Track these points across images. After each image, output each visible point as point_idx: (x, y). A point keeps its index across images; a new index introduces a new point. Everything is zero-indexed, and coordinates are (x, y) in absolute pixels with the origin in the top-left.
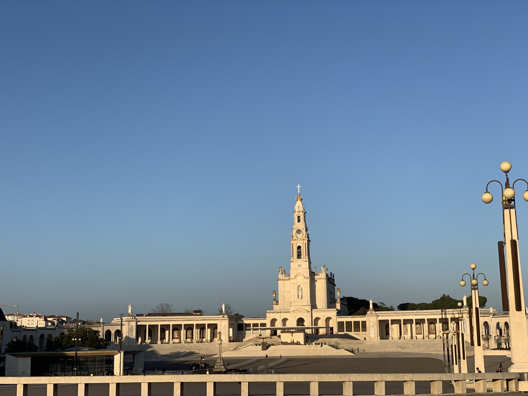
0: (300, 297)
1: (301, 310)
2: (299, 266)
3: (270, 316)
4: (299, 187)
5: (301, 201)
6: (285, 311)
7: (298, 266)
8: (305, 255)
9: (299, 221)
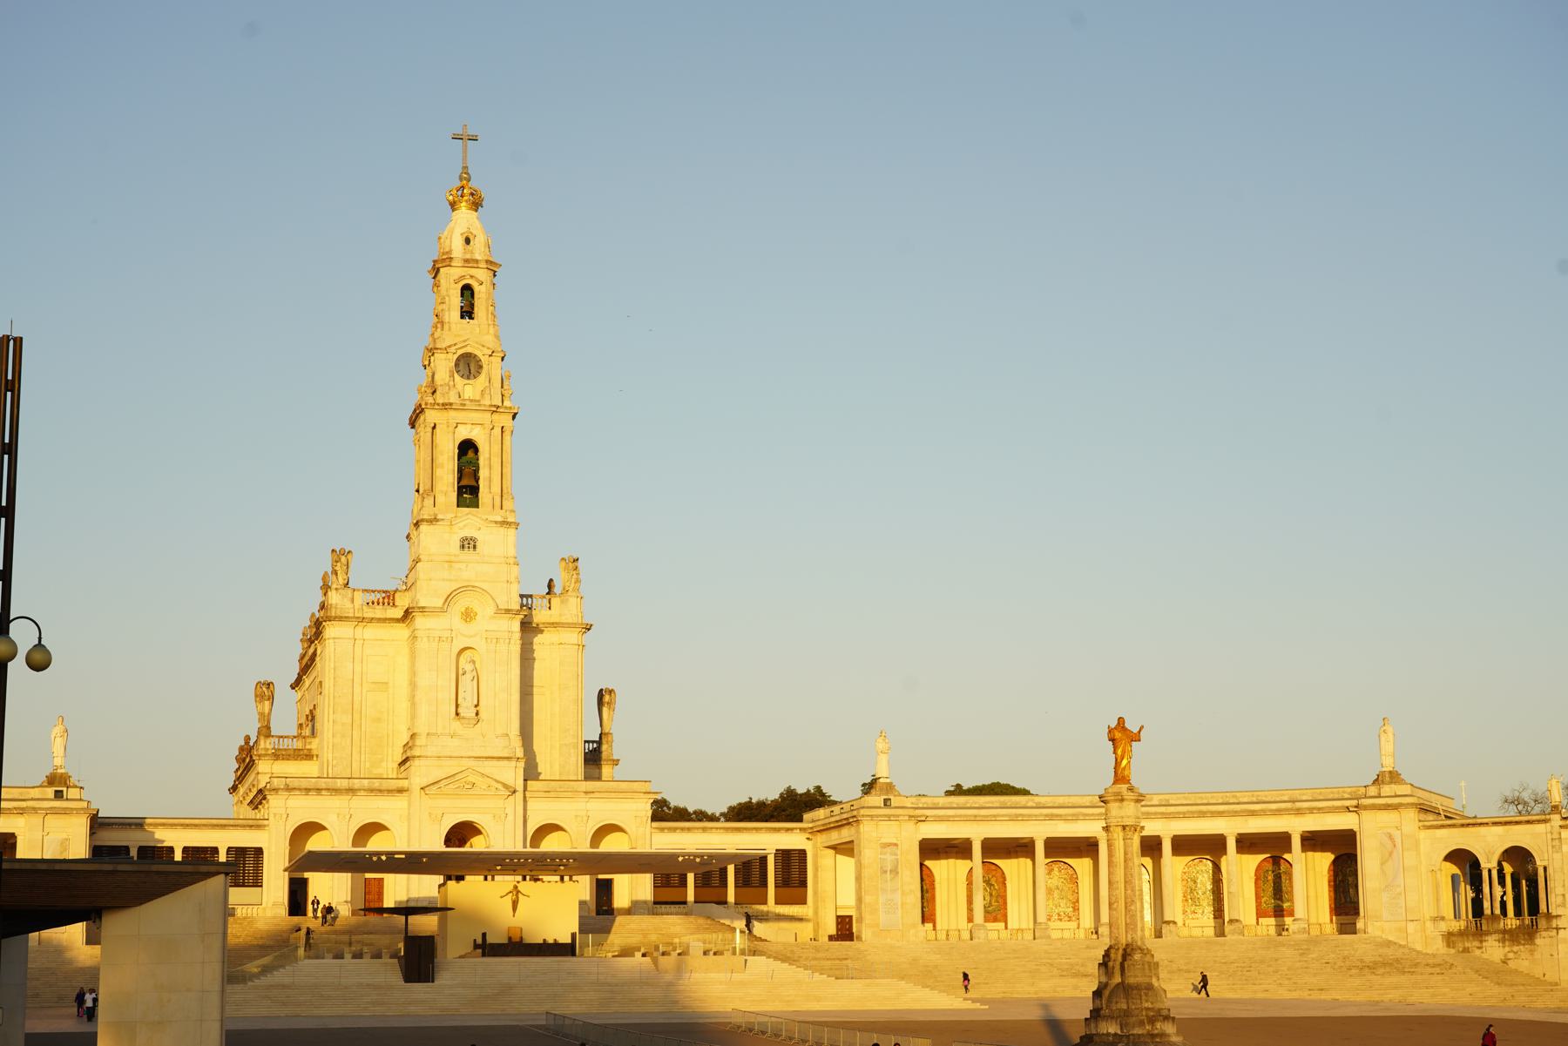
1: (471, 779)
2: (468, 544)
3: (285, 813)
5: (476, 211)
6: (376, 784)
7: (458, 544)
8: (496, 489)
9: (467, 313)
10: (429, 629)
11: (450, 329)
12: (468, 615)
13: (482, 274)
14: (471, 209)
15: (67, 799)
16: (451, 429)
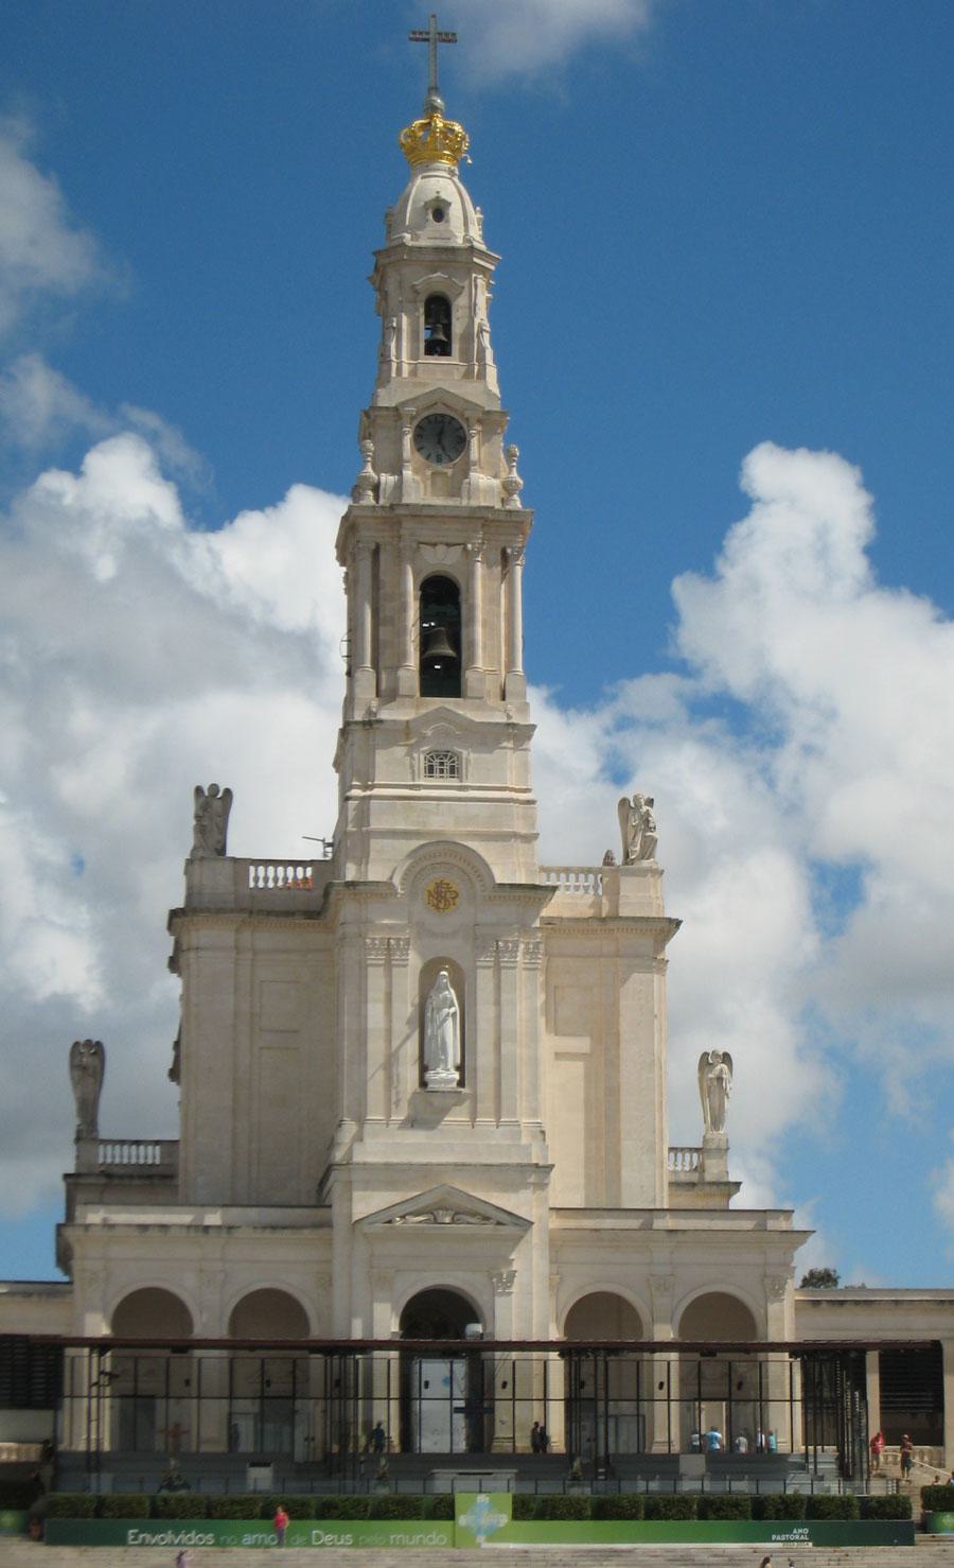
2: (444, 763)
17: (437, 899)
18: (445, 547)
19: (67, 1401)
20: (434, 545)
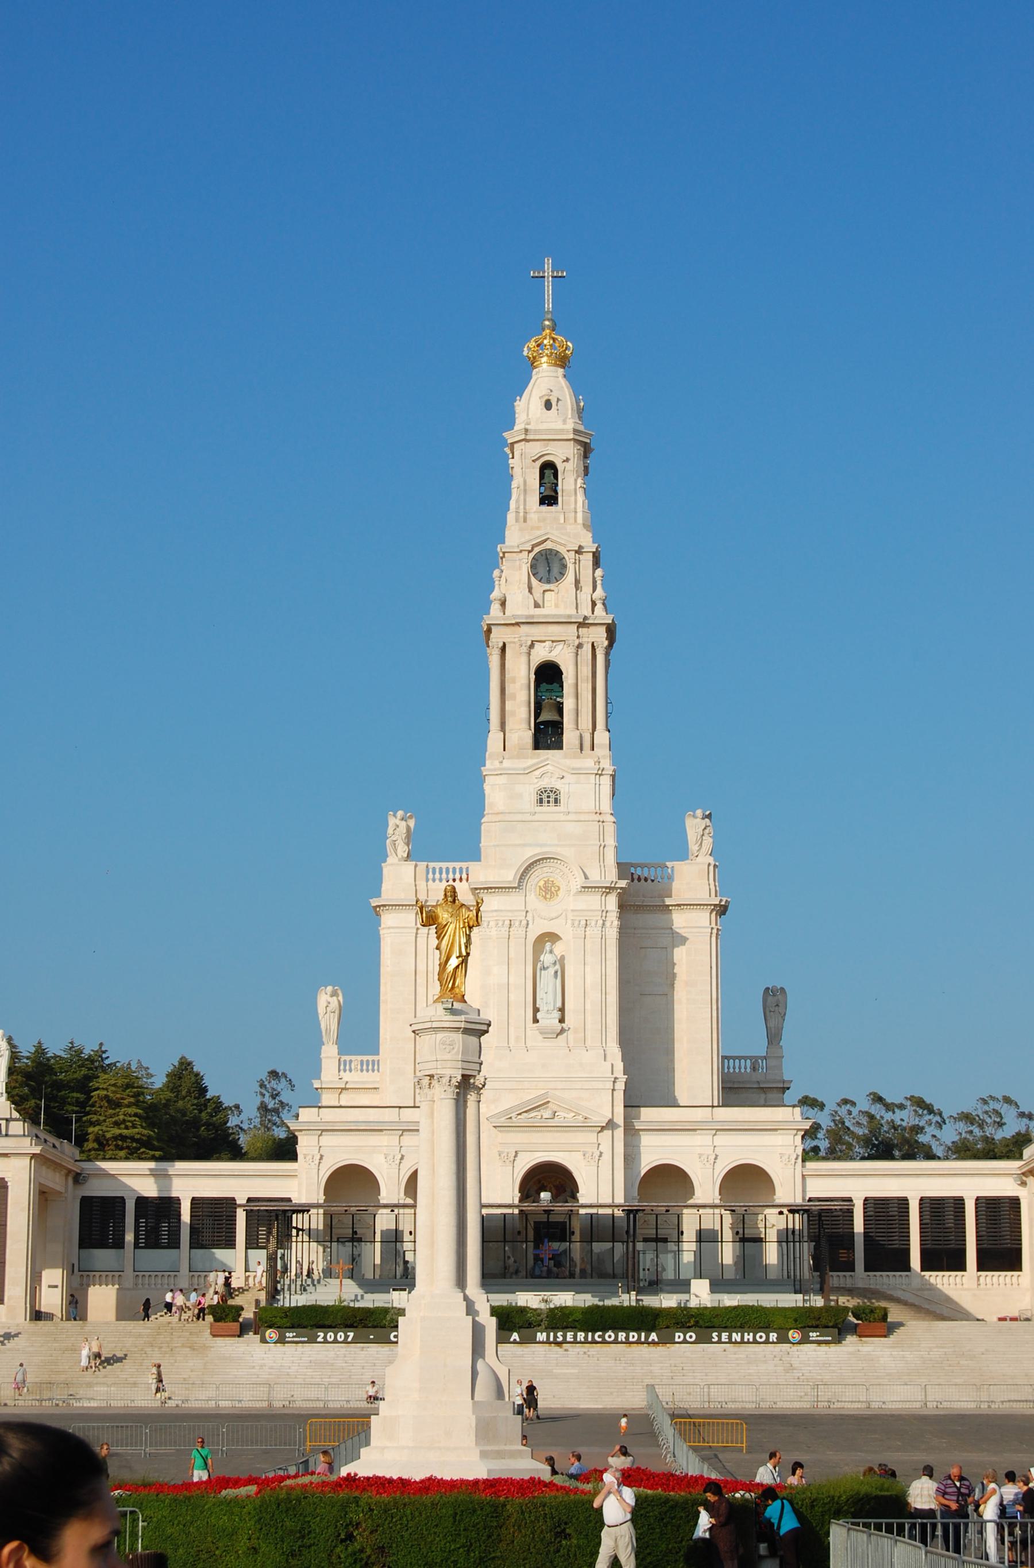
0: (549, 1019)
2: (548, 797)
4: (548, 272)
7: (534, 798)
9: (549, 499)
10: (496, 911)
11: (525, 521)
12: (549, 891)
13: (571, 451)
14: (556, 365)
15: (7, 1135)
16: (525, 649)
17: (545, 891)
18: (550, 642)
19: (294, 1244)
20: (544, 641)
